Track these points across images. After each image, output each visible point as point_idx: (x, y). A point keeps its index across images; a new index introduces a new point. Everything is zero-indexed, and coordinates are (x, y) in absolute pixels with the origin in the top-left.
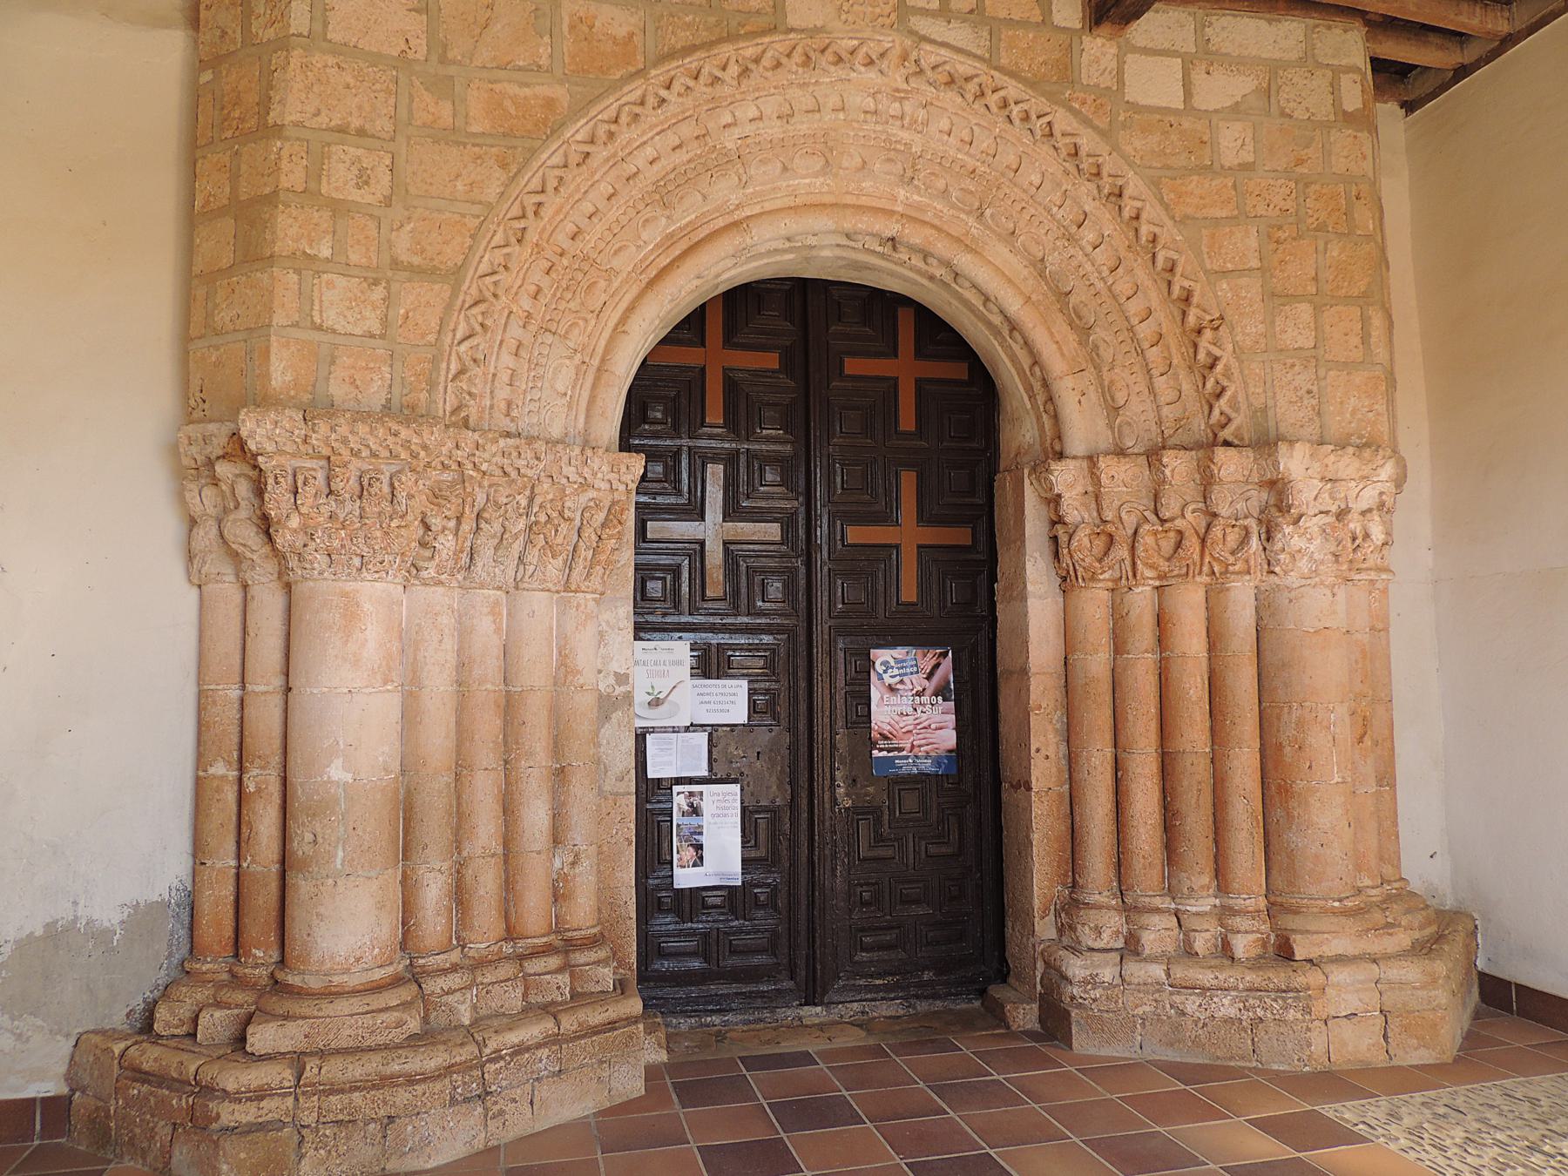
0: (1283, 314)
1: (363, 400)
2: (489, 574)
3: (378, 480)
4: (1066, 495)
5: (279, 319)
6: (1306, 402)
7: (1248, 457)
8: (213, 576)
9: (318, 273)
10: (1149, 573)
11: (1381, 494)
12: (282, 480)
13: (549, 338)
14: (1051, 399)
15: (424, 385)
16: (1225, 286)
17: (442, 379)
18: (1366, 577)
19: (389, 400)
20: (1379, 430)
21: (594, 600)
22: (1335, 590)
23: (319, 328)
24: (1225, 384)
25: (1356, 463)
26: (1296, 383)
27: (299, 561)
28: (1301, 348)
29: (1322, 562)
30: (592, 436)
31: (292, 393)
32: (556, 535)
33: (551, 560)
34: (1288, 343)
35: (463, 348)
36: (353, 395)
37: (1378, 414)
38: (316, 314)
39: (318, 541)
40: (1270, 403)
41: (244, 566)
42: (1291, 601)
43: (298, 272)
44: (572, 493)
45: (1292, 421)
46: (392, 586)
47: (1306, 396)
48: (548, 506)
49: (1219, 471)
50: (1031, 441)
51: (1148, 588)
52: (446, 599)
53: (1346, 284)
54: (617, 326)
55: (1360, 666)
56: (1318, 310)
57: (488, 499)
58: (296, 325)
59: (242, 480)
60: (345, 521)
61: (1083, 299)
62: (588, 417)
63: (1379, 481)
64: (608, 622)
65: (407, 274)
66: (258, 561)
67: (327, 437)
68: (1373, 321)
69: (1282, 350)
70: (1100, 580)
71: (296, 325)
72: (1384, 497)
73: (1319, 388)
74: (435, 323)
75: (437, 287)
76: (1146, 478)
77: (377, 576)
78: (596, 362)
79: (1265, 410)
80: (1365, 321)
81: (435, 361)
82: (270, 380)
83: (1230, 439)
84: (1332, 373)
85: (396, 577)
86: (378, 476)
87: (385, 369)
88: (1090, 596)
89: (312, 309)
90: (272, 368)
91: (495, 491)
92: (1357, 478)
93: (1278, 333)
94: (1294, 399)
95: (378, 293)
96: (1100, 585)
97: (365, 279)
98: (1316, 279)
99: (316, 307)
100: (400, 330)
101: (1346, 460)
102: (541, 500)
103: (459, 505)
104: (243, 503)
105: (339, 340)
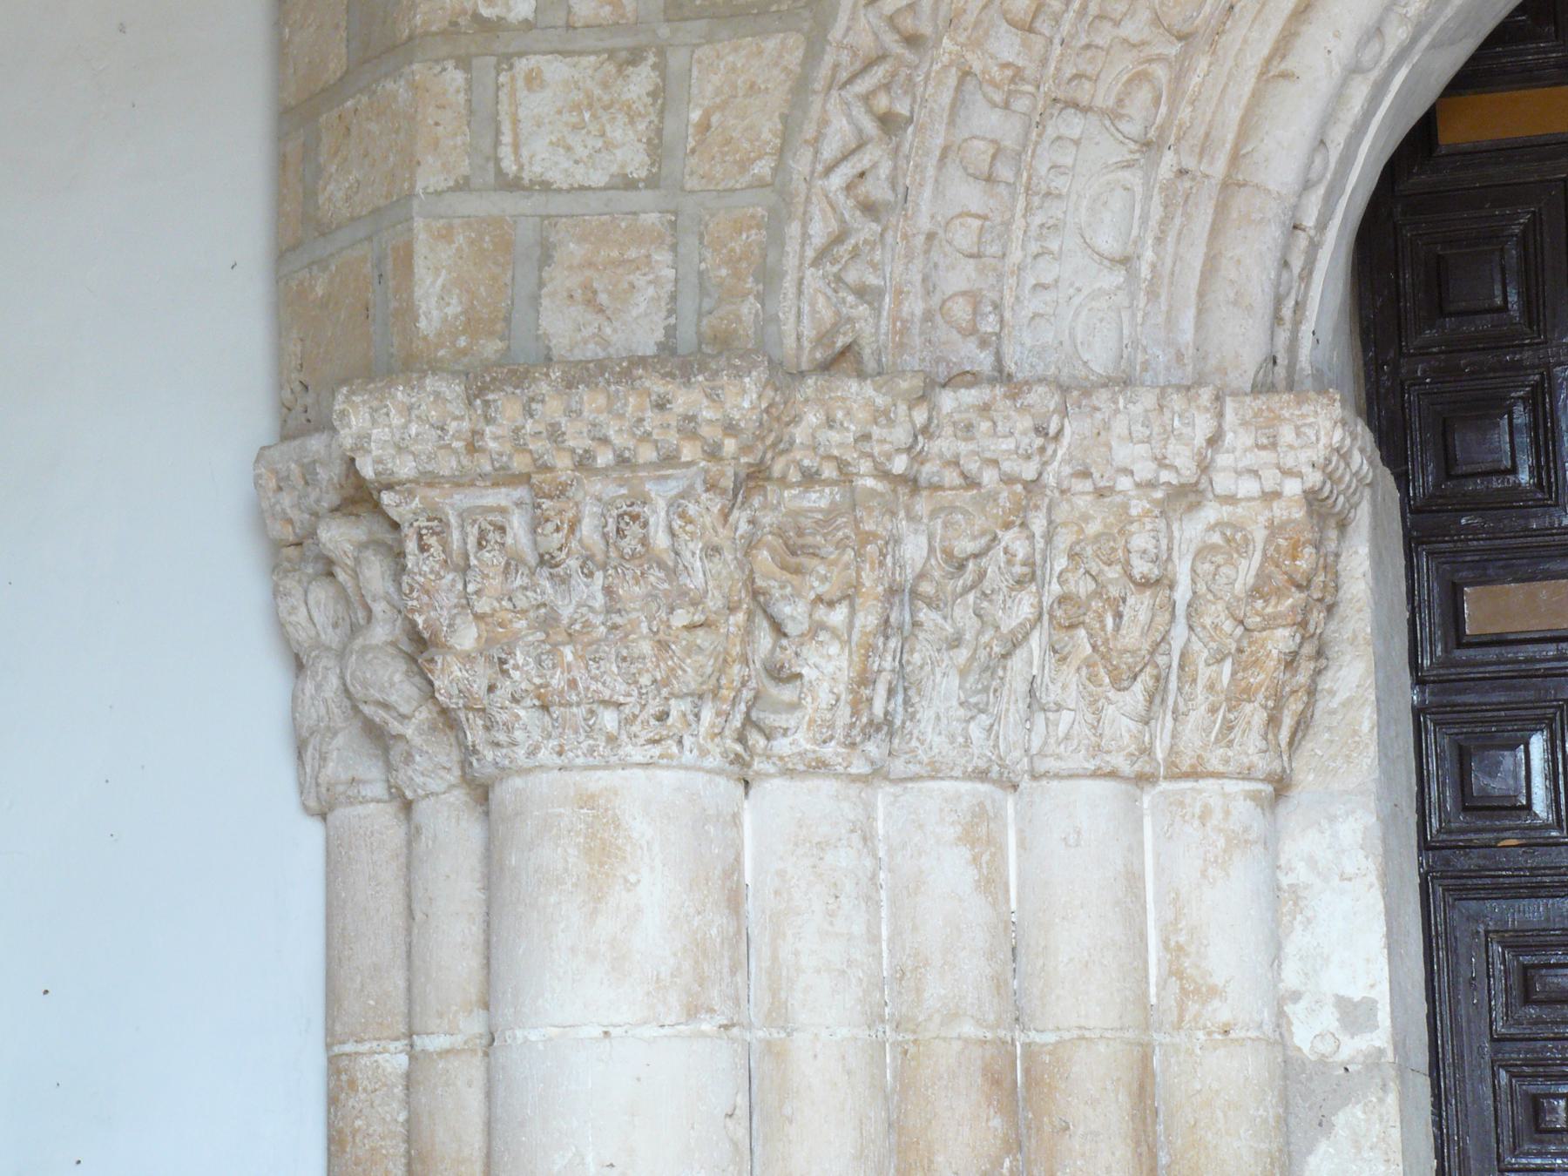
1: (614, 338)
2: (952, 738)
3: (635, 518)
5: (430, 178)
8: (341, 788)
9: (506, 60)
12: (433, 541)
13: (1073, 124)
15: (750, 283)
17: (791, 262)
19: (670, 331)
21: (1254, 797)
23: (512, 185)
27: (487, 729)
30: (1213, 362)
31: (462, 342)
32: (1117, 628)
33: (1112, 694)
35: (837, 180)
36: (592, 330)
38: (505, 152)
39: (516, 675)
41: (396, 754)
43: (464, 63)
44: (1147, 513)
46: (700, 779)
48: (1089, 551)
52: (846, 806)
54: (1268, 61)
57: (931, 550)
58: (463, 186)
59: (369, 554)
60: (573, 622)
62: (1200, 311)
64: (1312, 862)
65: (701, 25)
66: (417, 741)
67: (517, 431)
71: (463, 186)
74: (768, 130)
75: (771, 44)
77: (656, 751)
78: (1219, 168)
81: (774, 225)
82: (416, 319)
85: (704, 753)
86: (636, 509)
87: (662, 257)
89: (497, 143)
90: (418, 292)
91: (945, 526)
95: (641, 81)
97: (612, 53)
99: (507, 138)
100: (693, 161)
102: (1074, 538)
103: (847, 566)
104: (379, 608)
105: (558, 204)
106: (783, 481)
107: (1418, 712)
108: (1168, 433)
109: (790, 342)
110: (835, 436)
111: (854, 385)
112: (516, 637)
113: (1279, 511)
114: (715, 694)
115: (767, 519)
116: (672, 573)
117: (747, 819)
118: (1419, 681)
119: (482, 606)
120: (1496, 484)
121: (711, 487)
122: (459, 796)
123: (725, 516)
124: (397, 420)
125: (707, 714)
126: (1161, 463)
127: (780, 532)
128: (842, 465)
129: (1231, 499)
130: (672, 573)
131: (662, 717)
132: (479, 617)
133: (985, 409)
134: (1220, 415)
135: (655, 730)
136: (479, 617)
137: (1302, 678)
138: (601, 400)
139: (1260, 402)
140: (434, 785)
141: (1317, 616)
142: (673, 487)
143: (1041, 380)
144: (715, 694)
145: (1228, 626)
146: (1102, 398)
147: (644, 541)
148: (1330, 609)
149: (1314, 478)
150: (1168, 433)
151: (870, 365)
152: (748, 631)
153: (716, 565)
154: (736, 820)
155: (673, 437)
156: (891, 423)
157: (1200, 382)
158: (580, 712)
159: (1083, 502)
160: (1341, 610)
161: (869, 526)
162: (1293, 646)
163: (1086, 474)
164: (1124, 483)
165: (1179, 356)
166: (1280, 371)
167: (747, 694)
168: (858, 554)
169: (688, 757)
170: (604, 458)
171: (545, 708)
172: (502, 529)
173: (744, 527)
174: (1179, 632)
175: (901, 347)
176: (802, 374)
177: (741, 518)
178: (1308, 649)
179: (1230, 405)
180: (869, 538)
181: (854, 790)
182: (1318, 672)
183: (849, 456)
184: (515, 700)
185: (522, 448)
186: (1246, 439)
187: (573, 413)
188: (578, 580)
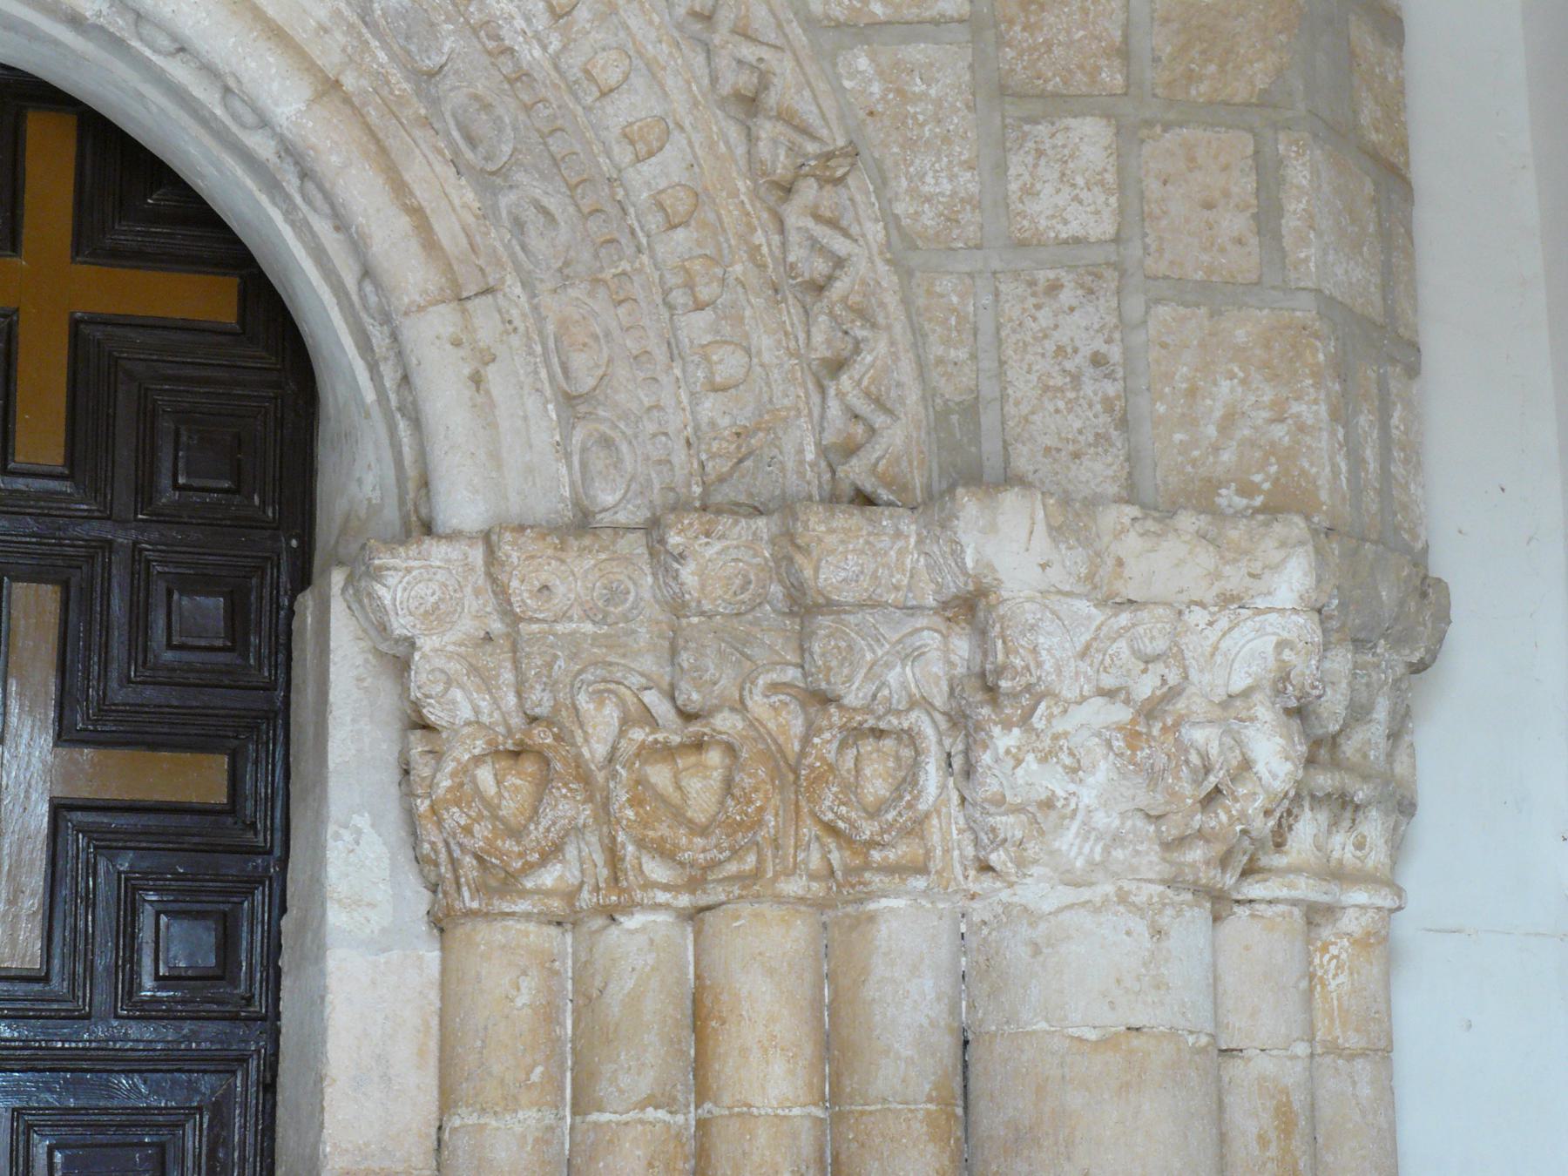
0: (1030, 145)
4: (427, 643)
6: (1088, 388)
7: (898, 534)
10: (657, 870)
11: (1281, 645)
14: (406, 380)
16: (863, 63)
18: (1284, 893)
20: (1303, 473)
22: (1164, 920)
24: (860, 333)
25: (1206, 558)
26: (1061, 337)
28: (1077, 241)
29: (1117, 839)
34: (1043, 223)
37: (1302, 428)
40: (989, 389)
42: (1036, 950)
45: (1049, 441)
47: (1089, 371)
49: (817, 569)
50: (375, 497)
51: (662, 917)
53: (1212, 68)
55: (1273, 1152)
56: (1128, 136)
61: (480, 88)
63: (1271, 610)
68: (1290, 172)
69: (1023, 244)
70: (524, 894)
72: (1287, 655)
73: (1126, 351)
76: (647, 595)
79: (971, 410)
80: (1268, 173)
83: (868, 486)
84: (1163, 311)
88: (500, 938)
92: (1209, 597)
93: (1014, 197)
94: (1059, 381)
96: (522, 906)
98: (1124, 53)
101: (1172, 548)
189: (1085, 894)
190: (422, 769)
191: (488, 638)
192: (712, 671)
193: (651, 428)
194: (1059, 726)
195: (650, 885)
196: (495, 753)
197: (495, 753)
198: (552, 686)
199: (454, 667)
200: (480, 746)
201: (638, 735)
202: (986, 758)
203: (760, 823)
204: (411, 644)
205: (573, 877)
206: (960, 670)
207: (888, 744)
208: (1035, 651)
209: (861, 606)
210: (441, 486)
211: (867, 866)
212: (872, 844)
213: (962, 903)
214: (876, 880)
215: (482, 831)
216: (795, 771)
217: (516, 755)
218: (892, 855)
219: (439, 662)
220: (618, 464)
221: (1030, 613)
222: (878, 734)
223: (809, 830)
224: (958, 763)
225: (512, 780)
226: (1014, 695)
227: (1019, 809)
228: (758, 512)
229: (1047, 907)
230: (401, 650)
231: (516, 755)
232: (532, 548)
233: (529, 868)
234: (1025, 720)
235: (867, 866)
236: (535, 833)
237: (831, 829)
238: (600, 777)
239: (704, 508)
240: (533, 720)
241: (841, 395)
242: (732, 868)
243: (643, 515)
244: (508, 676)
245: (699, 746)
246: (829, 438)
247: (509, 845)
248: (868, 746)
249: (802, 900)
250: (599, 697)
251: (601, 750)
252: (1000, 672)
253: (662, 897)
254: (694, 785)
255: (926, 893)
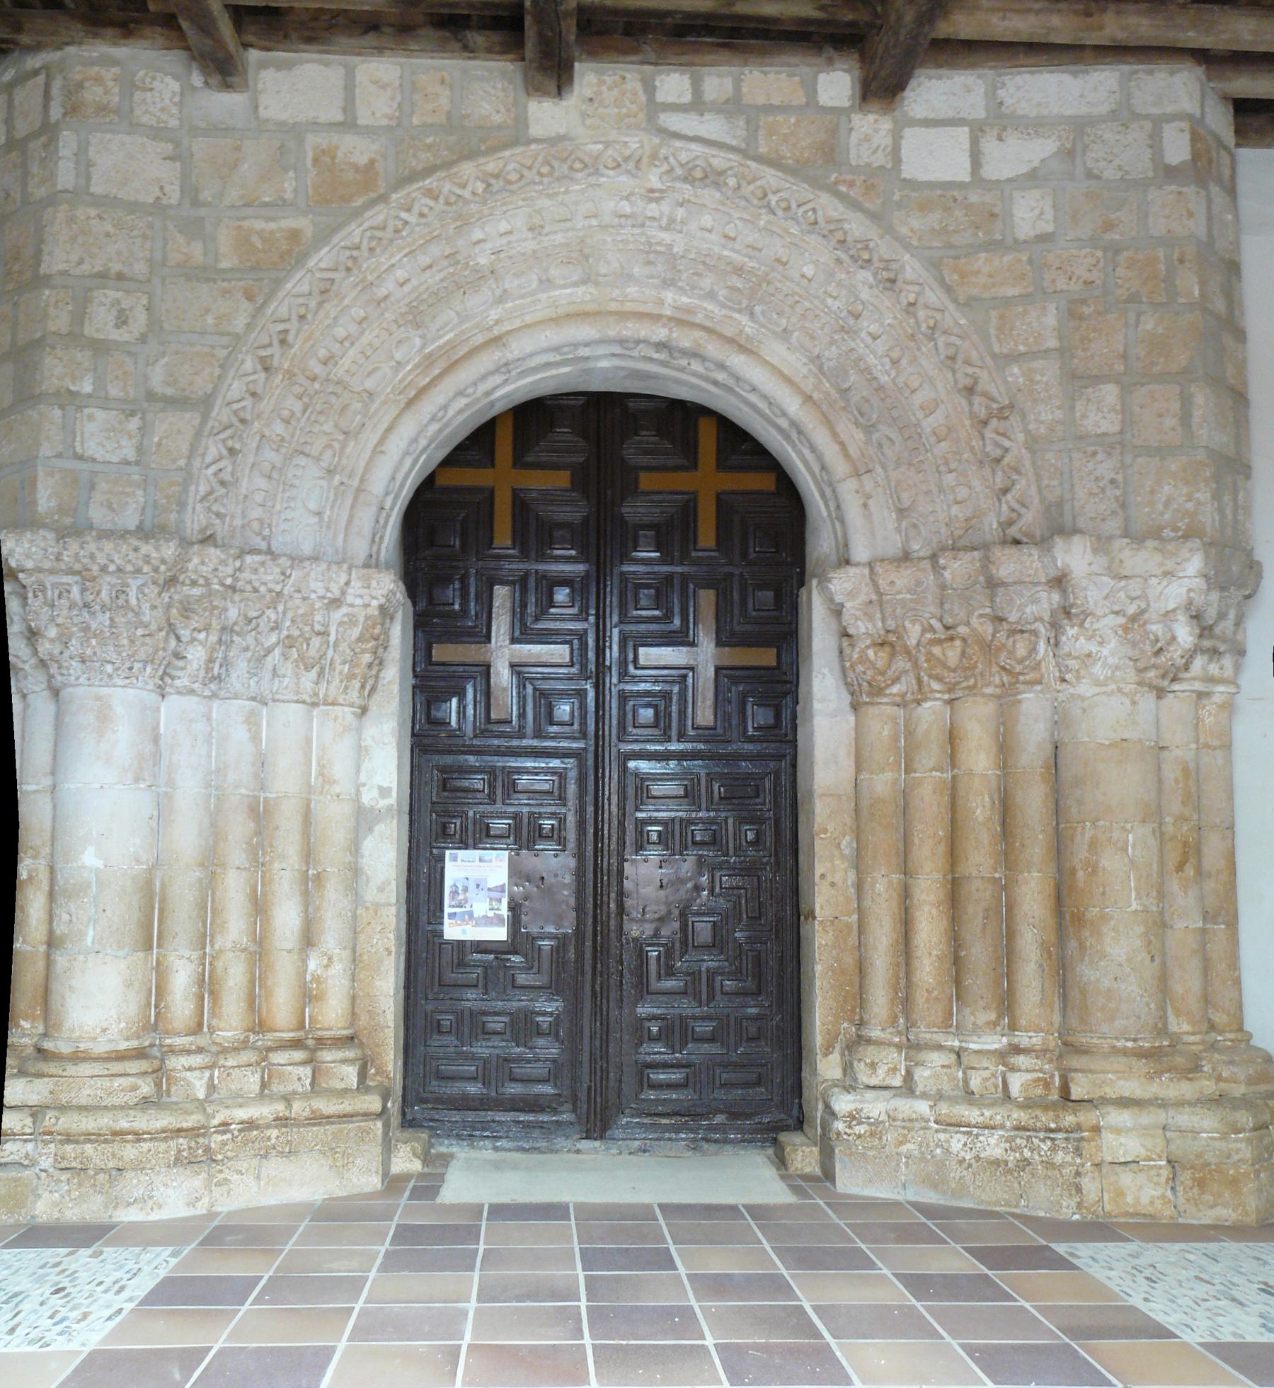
4: (848, 605)
5: (45, 451)
6: (1109, 492)
7: (1031, 555)
9: (80, 408)
10: (936, 686)
11: (1190, 590)
13: (302, 461)
14: (838, 507)
15: (174, 506)
16: (1016, 370)
17: (191, 500)
19: (142, 522)
21: (354, 713)
23: (80, 458)
24: (1015, 477)
25: (1158, 558)
28: (1104, 434)
29: (1117, 668)
31: (56, 517)
35: (210, 471)
37: (1199, 503)
38: (77, 444)
40: (1067, 496)
43: (62, 407)
46: (145, 693)
50: (828, 551)
51: (938, 703)
53: (1162, 359)
54: (376, 446)
58: (59, 456)
61: (865, 394)
62: (346, 536)
64: (373, 738)
65: (161, 405)
66: (30, 671)
67: (77, 554)
69: (1082, 437)
70: (886, 696)
71: (59, 456)
72: (1192, 594)
73: (1125, 478)
74: (185, 448)
75: (188, 415)
77: (127, 681)
78: (356, 483)
79: (1060, 504)
80: (1186, 402)
81: (185, 485)
83: (1018, 536)
84: (1141, 460)
87: (140, 493)
88: (877, 712)
89: (74, 441)
90: (39, 496)
94: (1096, 491)
95: (134, 423)
96: (885, 700)
97: (123, 410)
98: (1124, 357)
99: (78, 439)
100: (154, 457)
105: (98, 468)
106: (183, 583)
107: (414, 687)
108: (331, 579)
109: (189, 531)
110: (204, 568)
111: (212, 550)
112: (73, 634)
113: (370, 611)
114: (152, 661)
115: (176, 597)
116: (137, 614)
117: (163, 710)
118: (415, 676)
119: (59, 621)
120: (447, 608)
121: (154, 583)
122: (46, 693)
123: (160, 594)
124: (27, 546)
125: (149, 669)
126: (328, 590)
127: (181, 602)
128: (206, 579)
129: (352, 605)
130: (137, 614)
131: (131, 669)
132: (58, 625)
133: (263, 564)
134: (350, 575)
135: (127, 673)
136: (58, 625)
137: (374, 672)
138: (112, 545)
139: (365, 571)
140: (36, 688)
141: (380, 650)
142: (140, 582)
143: (285, 555)
144: (152, 661)
145: (348, 651)
146: (307, 564)
147: (127, 601)
148: (385, 648)
149: (383, 601)
150: (331, 579)
151: (220, 543)
152: (166, 640)
153: (155, 613)
154: (158, 710)
155: (140, 563)
156: (226, 565)
157: (344, 561)
158: (98, 664)
159: (298, 602)
160: (390, 649)
161: (215, 603)
162: (370, 660)
163: (299, 591)
164: (313, 596)
165: (337, 551)
166: (373, 560)
167: (165, 662)
168: (211, 613)
169: (140, 685)
170: (112, 568)
171: (83, 662)
172: (69, 592)
173: (167, 599)
174: (330, 653)
175: (232, 537)
176: (193, 544)
177: (166, 596)
178: (377, 662)
179: (354, 572)
180: (215, 608)
181: (204, 701)
182: (380, 671)
183: (210, 576)
184: (71, 658)
185: (78, 561)
186: (359, 584)
187: (100, 550)
188: (100, 615)
189: (1104, 689)
190: (847, 651)
191: (871, 602)
192: (956, 611)
193: (931, 519)
194: (1096, 626)
195: (933, 691)
196: (874, 644)
197: (874, 644)
198: (895, 618)
199: (858, 613)
200: (868, 642)
201: (928, 636)
202: (1064, 639)
203: (976, 667)
204: (842, 605)
205: (904, 688)
206: (1055, 606)
207: (1026, 635)
208: (1086, 597)
209: (1015, 583)
210: (852, 546)
211: (1018, 682)
212: (1020, 674)
213: (1055, 694)
214: (1022, 687)
215: (870, 673)
216: (989, 646)
217: (882, 645)
218: (1027, 677)
219: (853, 611)
220: (919, 534)
221: (1084, 583)
222: (1022, 632)
223: (995, 669)
224: (1052, 641)
225: (881, 654)
226: (1077, 615)
227: (1077, 658)
228: (974, 549)
229: (1088, 695)
230: (839, 608)
231: (882, 645)
232: (888, 567)
233: (888, 686)
234: (1081, 625)
235: (1018, 682)
236: (890, 673)
237: (1004, 668)
238: (914, 652)
239: (953, 549)
240: (888, 631)
241: (1007, 502)
242: (965, 684)
243: (929, 553)
244: (878, 615)
245: (952, 639)
246: (1002, 519)
247: (880, 678)
248: (1018, 637)
249: (992, 695)
250: (913, 622)
251: (914, 642)
252: (1072, 606)
253: (938, 695)
254: (950, 653)
255: (1041, 691)
